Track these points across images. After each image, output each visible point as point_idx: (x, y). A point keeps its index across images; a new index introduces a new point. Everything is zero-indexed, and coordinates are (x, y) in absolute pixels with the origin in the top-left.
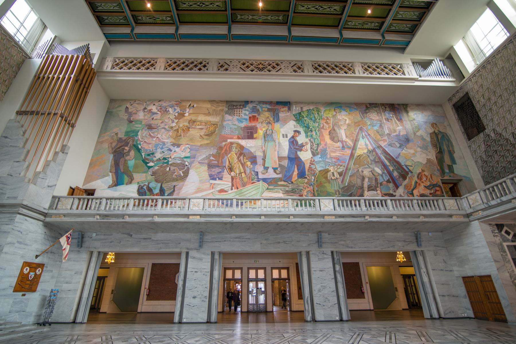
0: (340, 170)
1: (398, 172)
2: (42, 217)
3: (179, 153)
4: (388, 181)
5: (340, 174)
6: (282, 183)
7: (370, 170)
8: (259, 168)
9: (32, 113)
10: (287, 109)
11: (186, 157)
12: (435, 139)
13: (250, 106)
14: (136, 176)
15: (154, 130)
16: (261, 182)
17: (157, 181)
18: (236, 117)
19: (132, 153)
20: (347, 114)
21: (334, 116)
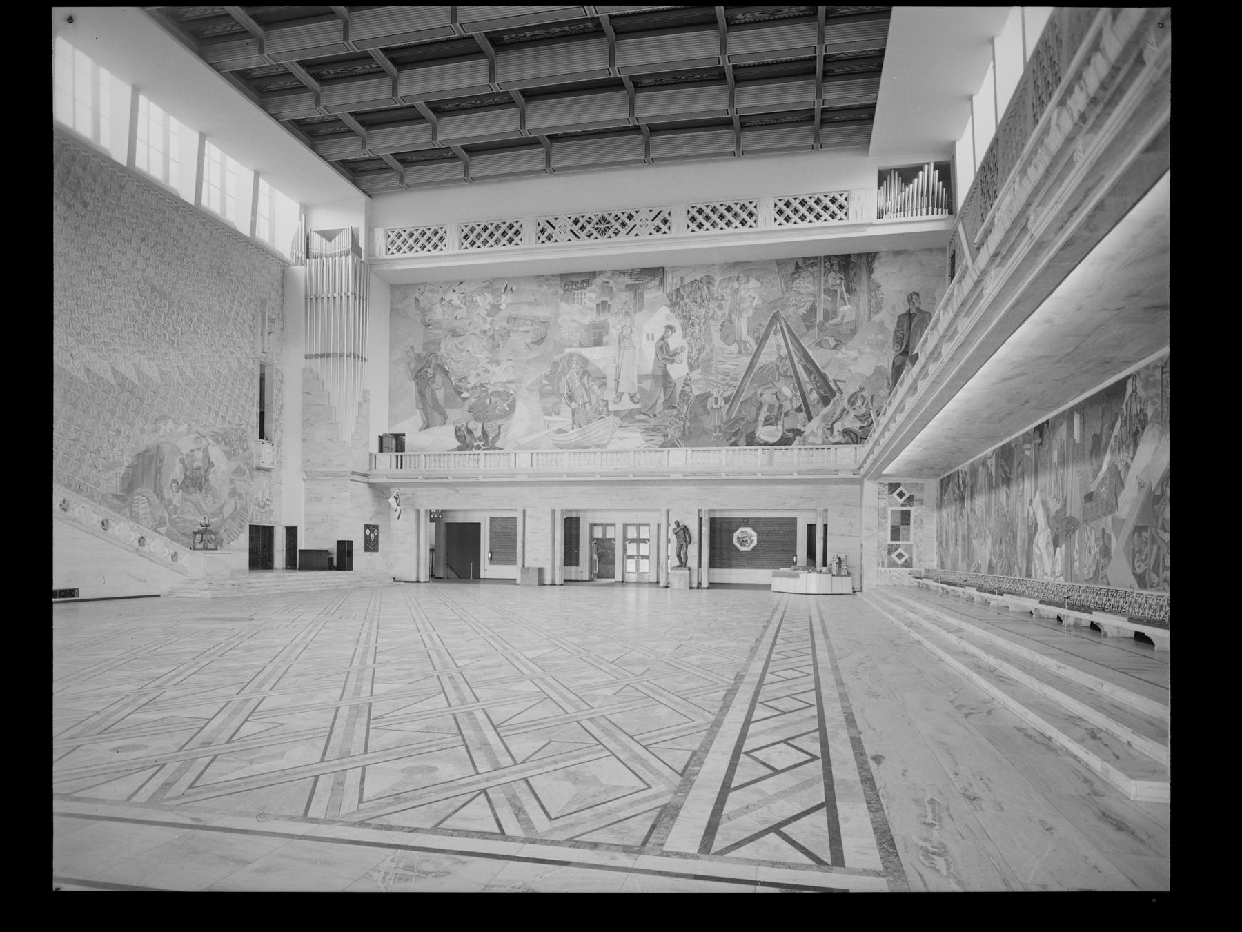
0: (726, 394)
1: (819, 394)
2: (364, 479)
3: (499, 376)
4: (799, 410)
5: (726, 400)
6: (641, 417)
7: (774, 391)
8: (610, 395)
9: (322, 356)
10: (656, 282)
11: (509, 382)
12: (905, 327)
13: (599, 280)
14: (448, 411)
15: (461, 339)
16: (612, 416)
17: (476, 419)
18: (577, 307)
19: (439, 378)
20: (759, 284)
21: (735, 292)
